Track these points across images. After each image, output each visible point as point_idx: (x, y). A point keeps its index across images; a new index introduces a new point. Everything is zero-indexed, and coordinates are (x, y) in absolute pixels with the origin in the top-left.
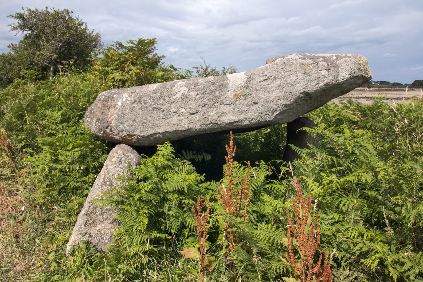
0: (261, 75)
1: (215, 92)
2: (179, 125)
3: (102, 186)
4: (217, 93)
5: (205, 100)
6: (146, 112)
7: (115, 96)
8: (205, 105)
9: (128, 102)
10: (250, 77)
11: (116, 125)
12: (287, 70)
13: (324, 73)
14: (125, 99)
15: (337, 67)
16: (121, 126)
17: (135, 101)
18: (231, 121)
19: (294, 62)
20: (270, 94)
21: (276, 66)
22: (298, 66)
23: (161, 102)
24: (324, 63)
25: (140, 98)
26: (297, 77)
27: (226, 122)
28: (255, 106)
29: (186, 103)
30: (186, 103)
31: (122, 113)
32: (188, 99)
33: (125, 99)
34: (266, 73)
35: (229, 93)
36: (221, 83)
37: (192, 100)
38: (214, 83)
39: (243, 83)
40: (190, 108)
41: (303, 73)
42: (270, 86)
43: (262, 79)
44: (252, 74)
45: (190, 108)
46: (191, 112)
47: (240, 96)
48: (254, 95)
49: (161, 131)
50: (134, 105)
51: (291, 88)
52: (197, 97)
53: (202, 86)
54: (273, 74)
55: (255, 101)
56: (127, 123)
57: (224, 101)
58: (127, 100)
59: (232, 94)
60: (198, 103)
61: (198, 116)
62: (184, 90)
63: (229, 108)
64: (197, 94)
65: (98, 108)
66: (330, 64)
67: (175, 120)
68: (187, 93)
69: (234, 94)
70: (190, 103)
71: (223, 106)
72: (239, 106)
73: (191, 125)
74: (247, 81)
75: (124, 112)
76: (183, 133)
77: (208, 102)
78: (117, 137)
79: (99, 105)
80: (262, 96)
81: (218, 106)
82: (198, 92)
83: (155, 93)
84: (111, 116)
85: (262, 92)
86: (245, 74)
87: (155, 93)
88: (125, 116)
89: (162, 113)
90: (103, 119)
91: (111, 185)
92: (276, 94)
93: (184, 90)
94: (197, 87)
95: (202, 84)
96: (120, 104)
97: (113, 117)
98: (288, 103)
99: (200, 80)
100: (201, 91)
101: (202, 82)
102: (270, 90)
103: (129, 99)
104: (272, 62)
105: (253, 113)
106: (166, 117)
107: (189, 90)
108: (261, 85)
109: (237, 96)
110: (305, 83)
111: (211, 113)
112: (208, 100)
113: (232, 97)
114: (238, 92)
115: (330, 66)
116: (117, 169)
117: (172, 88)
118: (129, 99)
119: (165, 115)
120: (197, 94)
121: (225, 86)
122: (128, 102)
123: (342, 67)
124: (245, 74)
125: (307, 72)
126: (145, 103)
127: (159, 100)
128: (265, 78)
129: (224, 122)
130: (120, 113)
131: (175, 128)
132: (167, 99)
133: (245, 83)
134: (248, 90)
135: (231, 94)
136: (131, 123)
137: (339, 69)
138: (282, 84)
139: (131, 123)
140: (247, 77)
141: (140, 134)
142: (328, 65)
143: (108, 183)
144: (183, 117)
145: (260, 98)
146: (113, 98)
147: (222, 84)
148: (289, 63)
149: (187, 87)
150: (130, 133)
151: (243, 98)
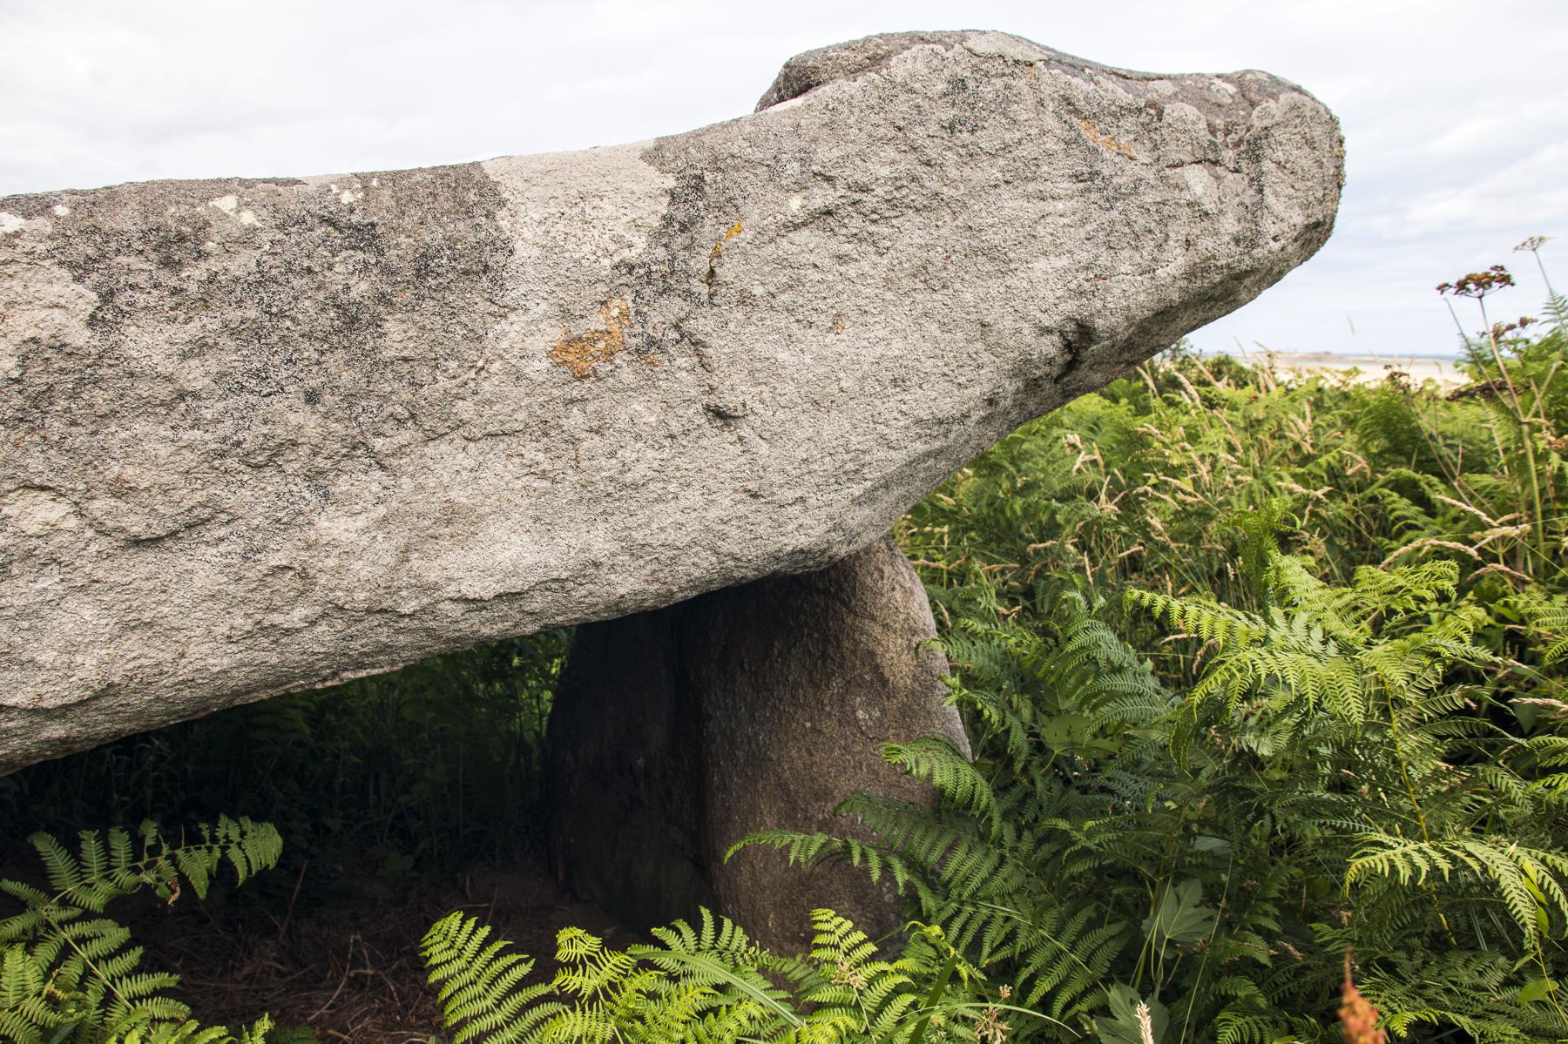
0: (794, 168)
1: (377, 322)
4: (397, 335)
5: (279, 404)
8: (278, 450)
10: (698, 184)
12: (985, 140)
13: (1198, 180)
15: (1253, 150)
18: (516, 584)
19: (1021, 84)
22: (1050, 122)
24: (1190, 111)
26: (1049, 206)
28: (719, 445)
29: (79, 438)
30: (79, 438)
32: (100, 399)
34: (826, 154)
35: (510, 332)
36: (433, 236)
37: (146, 407)
38: (365, 236)
39: (641, 242)
40: (121, 490)
41: (1077, 177)
42: (851, 270)
43: (795, 203)
44: (716, 163)
45: (121, 490)
46: (137, 525)
47: (610, 354)
48: (717, 349)
51: (995, 287)
52: (195, 375)
53: (242, 264)
54: (882, 167)
55: (729, 401)
57: (465, 409)
59: (539, 344)
60: (209, 439)
61: (204, 567)
63: (501, 471)
64: (198, 348)
66: (1219, 122)
68: (80, 337)
69: (554, 334)
70: (116, 434)
71: (450, 458)
72: (591, 443)
73: (133, 643)
74: (668, 220)
76: (56, 731)
77: (307, 422)
80: (783, 356)
81: (400, 451)
85: (782, 320)
94: (196, 273)
95: (248, 238)
98: (947, 407)
100: (234, 315)
101: (248, 218)
102: (848, 304)
104: (861, 69)
105: (694, 497)
107: (107, 297)
108: (782, 263)
109: (578, 358)
110: (1084, 257)
111: (334, 526)
112: (312, 398)
113: (538, 367)
114: (597, 322)
115: (1220, 138)
120: (198, 348)
121: (483, 266)
123: (1280, 156)
125: (1106, 172)
128: (822, 197)
129: (451, 590)
134: (675, 307)
135: (527, 335)
137: (1267, 165)
138: (937, 257)
140: (670, 182)
142: (1213, 130)
144: (50, 581)
145: (762, 371)
147: (451, 242)
148: (988, 92)
149: (80, 270)
151: (627, 376)
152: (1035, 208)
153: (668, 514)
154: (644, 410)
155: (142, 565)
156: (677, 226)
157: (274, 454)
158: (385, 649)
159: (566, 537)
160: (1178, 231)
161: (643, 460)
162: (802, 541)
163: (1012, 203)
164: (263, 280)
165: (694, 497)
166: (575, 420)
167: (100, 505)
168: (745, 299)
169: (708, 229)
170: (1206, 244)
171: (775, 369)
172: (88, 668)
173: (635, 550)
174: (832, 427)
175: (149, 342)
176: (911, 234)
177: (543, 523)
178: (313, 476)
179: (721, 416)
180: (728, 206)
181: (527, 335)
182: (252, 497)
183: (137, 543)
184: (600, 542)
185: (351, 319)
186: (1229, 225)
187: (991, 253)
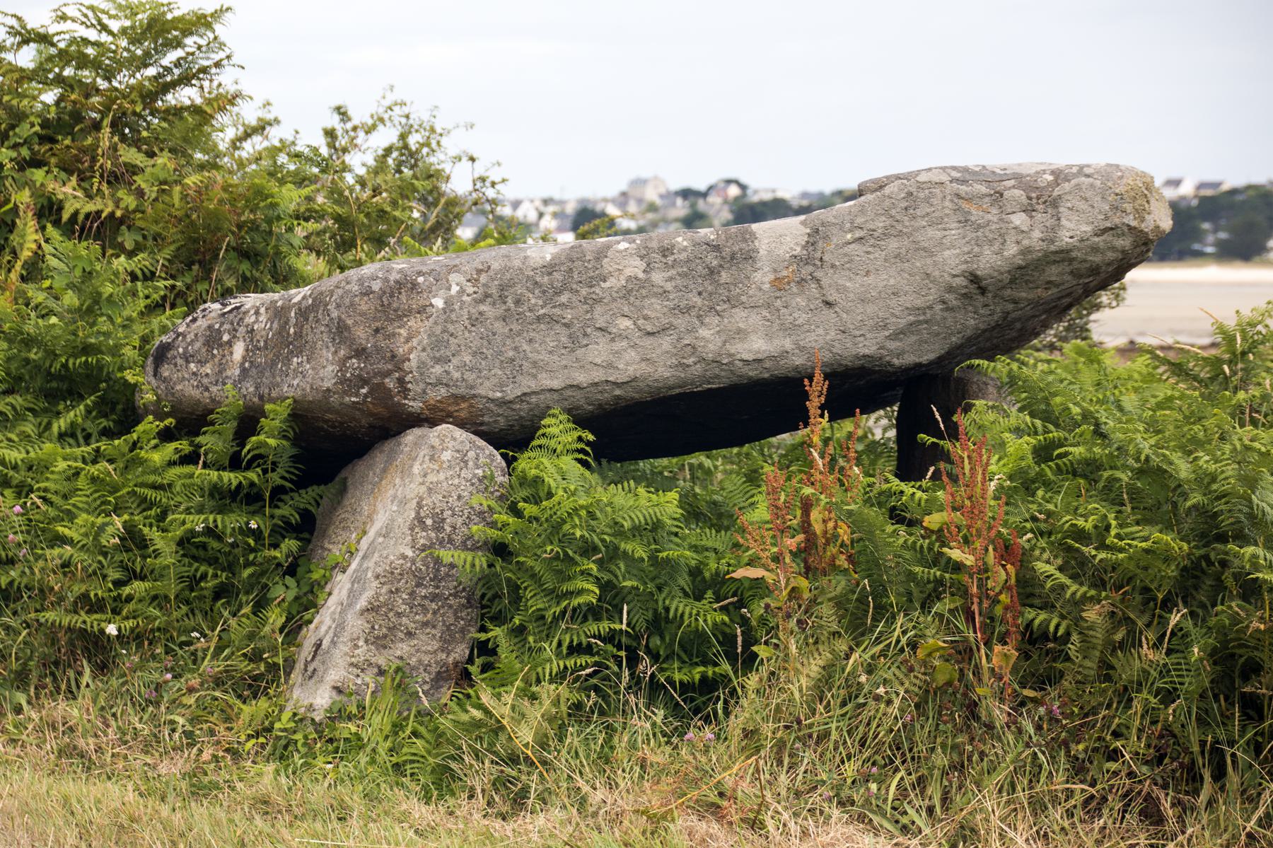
0: (848, 225)
1: (719, 272)
2: (610, 365)
3: (412, 529)
4: (724, 276)
5: (690, 295)
6: (516, 327)
7: (421, 279)
8: (689, 309)
9: (465, 298)
10: (817, 231)
11: (422, 365)
12: (918, 212)
13: (1019, 219)
14: (455, 289)
15: (1054, 203)
16: (438, 370)
17: (487, 296)
18: (760, 356)
19: (937, 191)
20: (871, 279)
21: (887, 203)
22: (947, 204)
23: (564, 298)
24: (1018, 193)
25: (502, 288)
26: (947, 233)
27: (746, 356)
28: (828, 314)
29: (638, 303)
30: (638, 303)
31: (444, 331)
32: (644, 292)
33: (455, 289)
34: (859, 220)
35: (757, 276)
36: (736, 248)
37: (656, 295)
38: (717, 248)
39: (799, 249)
40: (646, 318)
41: (960, 222)
42: (871, 257)
43: (849, 236)
44: (823, 224)
45: (646, 318)
47: (789, 283)
49: (556, 384)
50: (482, 308)
51: (929, 261)
52: (669, 286)
53: (683, 256)
54: (880, 224)
55: (830, 299)
56: (455, 361)
57: (744, 298)
58: (462, 291)
59: (766, 279)
60: (671, 304)
61: (666, 343)
62: (635, 267)
63: (755, 319)
64: (671, 279)
65: (362, 314)
66: (1034, 195)
67: (599, 351)
68: (641, 275)
69: (772, 277)
71: (739, 313)
72: (783, 311)
73: (643, 365)
74: (807, 242)
75: (451, 328)
76: (618, 392)
77: (698, 300)
78: (415, 405)
79: (364, 307)
80: (848, 284)
81: (724, 311)
82: (673, 272)
83: (550, 274)
84: (408, 340)
85: (847, 273)
86: (803, 223)
87: (550, 274)
88: (452, 340)
89: (564, 331)
90: (378, 349)
91: (438, 528)
92: (887, 278)
93: (635, 267)
94: (671, 258)
95: (685, 249)
96: (439, 303)
97: (415, 342)
99: (680, 239)
100: (680, 270)
101: (685, 243)
102: (871, 268)
103: (470, 290)
104: (876, 190)
105: (820, 331)
106: (575, 342)
107: (648, 265)
108: (846, 255)
109: (778, 284)
110: (966, 249)
111: (704, 332)
112: (700, 294)
113: (767, 286)
114: (785, 273)
115: (1034, 201)
116: (456, 481)
117: (598, 259)
118: (470, 290)
119: (570, 336)
120: (671, 279)
121: (750, 257)
122: (465, 298)
123: (1069, 205)
124: (803, 223)
125: (973, 219)
126: (518, 302)
127: (558, 293)
128: (858, 234)
129: (738, 357)
130: (438, 329)
131: (598, 375)
132: (584, 292)
133: (804, 247)
134: (810, 268)
135: (763, 277)
136: (467, 359)
137: (1061, 209)
138: (903, 251)
139: (467, 359)
140: (808, 231)
141: (491, 395)
142: (1030, 198)
143: (429, 522)
144: (624, 343)
145: (841, 289)
146: (414, 285)
147: (741, 250)
148: (922, 195)
149: (642, 258)
150: (462, 391)
151: (795, 290)
152: (940, 234)
153: (812, 337)
154: (799, 300)
155: (648, 342)
156: (811, 244)
157: (689, 309)
158: (717, 376)
159: (777, 342)
160: (1011, 239)
161: (802, 318)
162: (867, 352)
163: (931, 232)
164: (689, 260)
165: (820, 331)
166: (778, 303)
167: (640, 322)
168: (833, 266)
169: (820, 244)
170: (1026, 242)
171: (846, 289)
172: (631, 371)
173: (802, 349)
174: (871, 309)
175: (658, 277)
176: (893, 244)
177: (769, 337)
178: (699, 317)
179: (829, 304)
180: (826, 238)
181: (763, 277)
182: (681, 322)
183: (649, 334)
184: (788, 344)
185: (712, 272)
186: (1037, 234)
187: (924, 249)
